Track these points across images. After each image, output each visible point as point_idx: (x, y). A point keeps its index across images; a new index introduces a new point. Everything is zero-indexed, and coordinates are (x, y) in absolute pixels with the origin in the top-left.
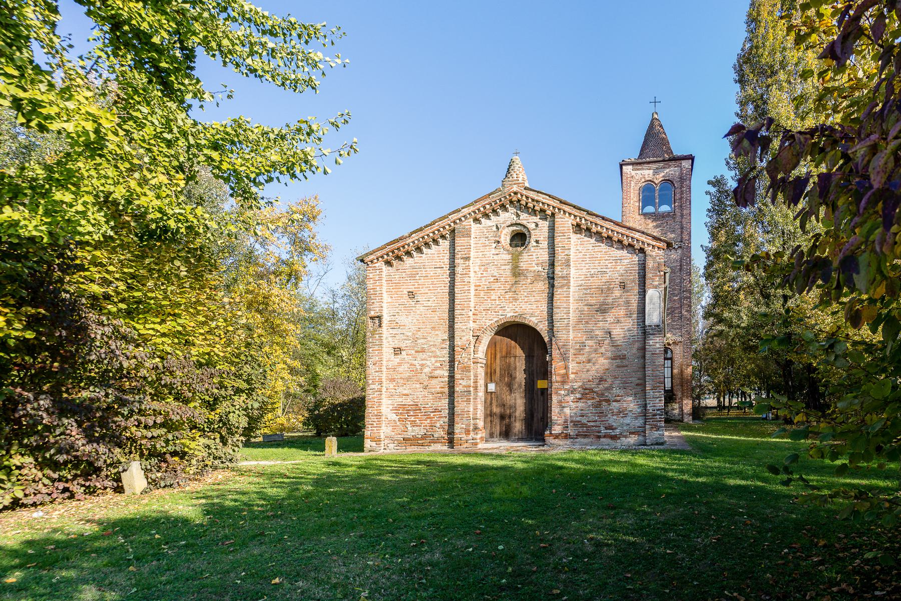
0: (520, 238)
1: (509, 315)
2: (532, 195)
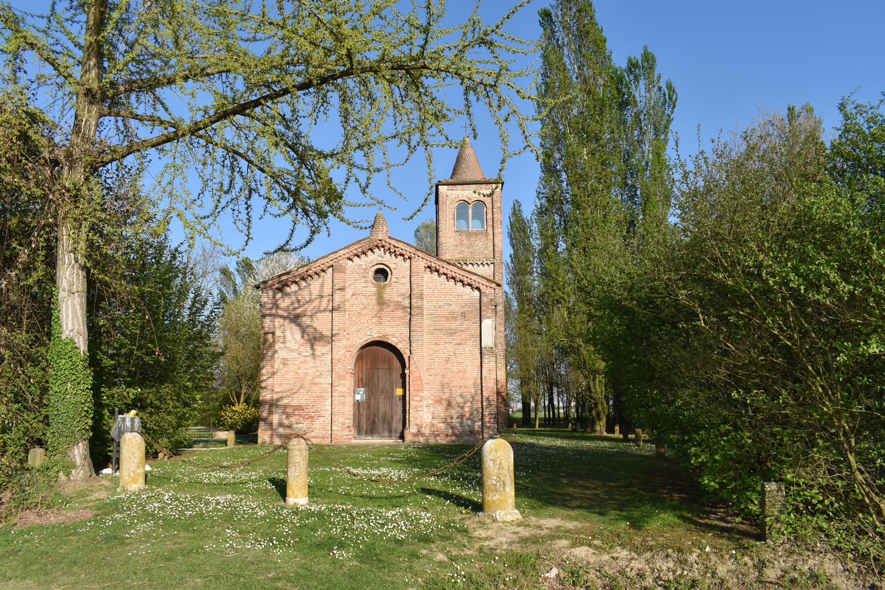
0: (382, 273)
1: (376, 335)
2: (393, 242)
